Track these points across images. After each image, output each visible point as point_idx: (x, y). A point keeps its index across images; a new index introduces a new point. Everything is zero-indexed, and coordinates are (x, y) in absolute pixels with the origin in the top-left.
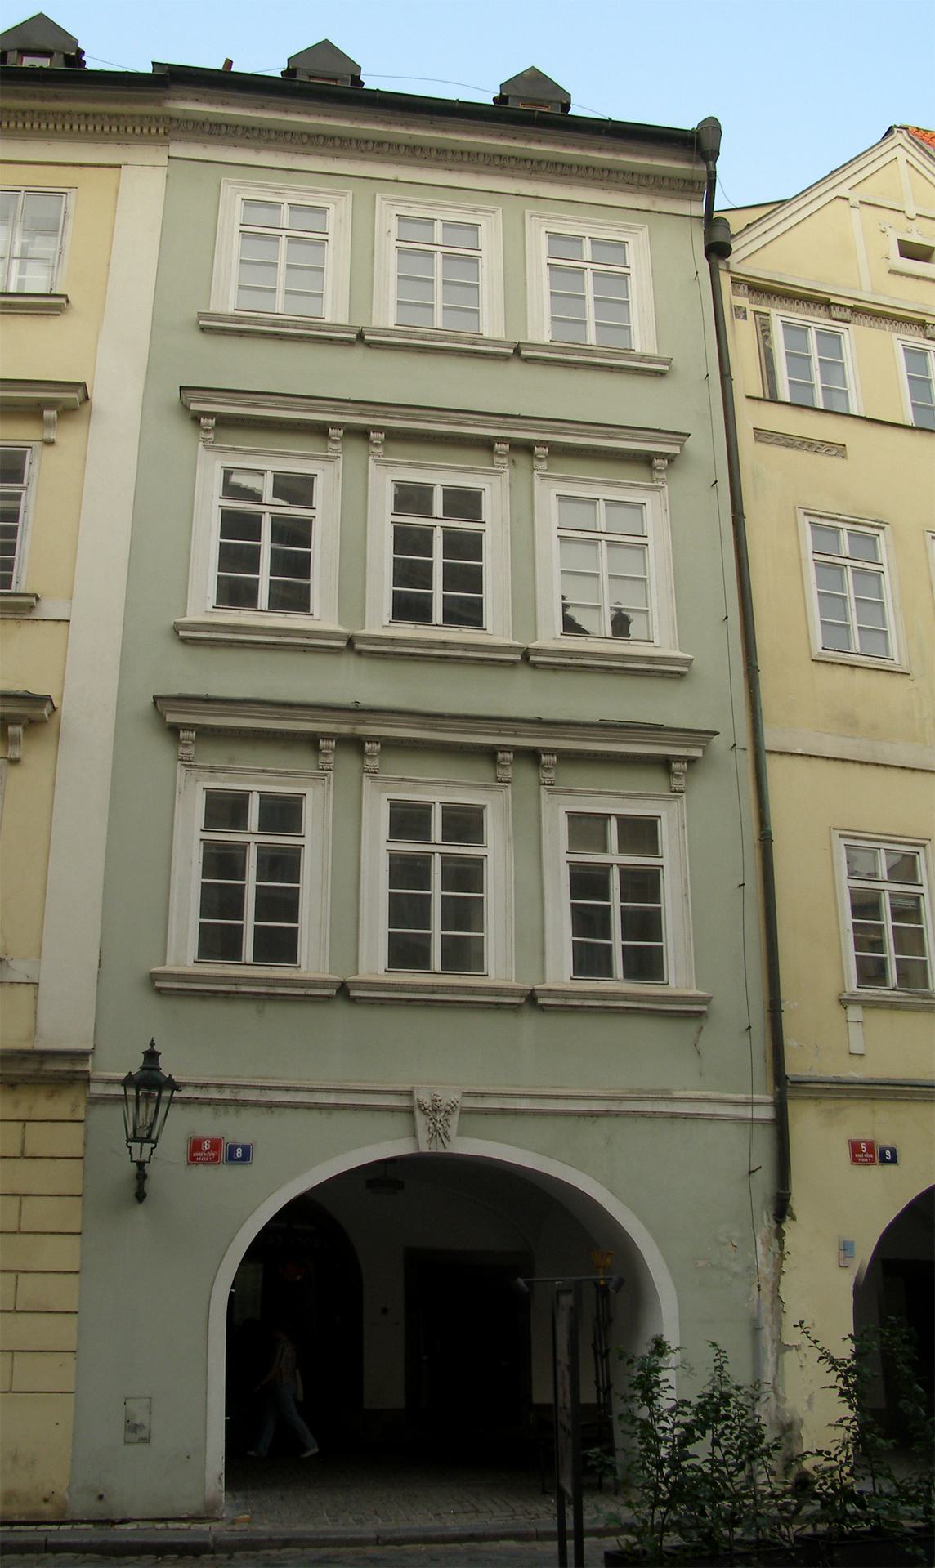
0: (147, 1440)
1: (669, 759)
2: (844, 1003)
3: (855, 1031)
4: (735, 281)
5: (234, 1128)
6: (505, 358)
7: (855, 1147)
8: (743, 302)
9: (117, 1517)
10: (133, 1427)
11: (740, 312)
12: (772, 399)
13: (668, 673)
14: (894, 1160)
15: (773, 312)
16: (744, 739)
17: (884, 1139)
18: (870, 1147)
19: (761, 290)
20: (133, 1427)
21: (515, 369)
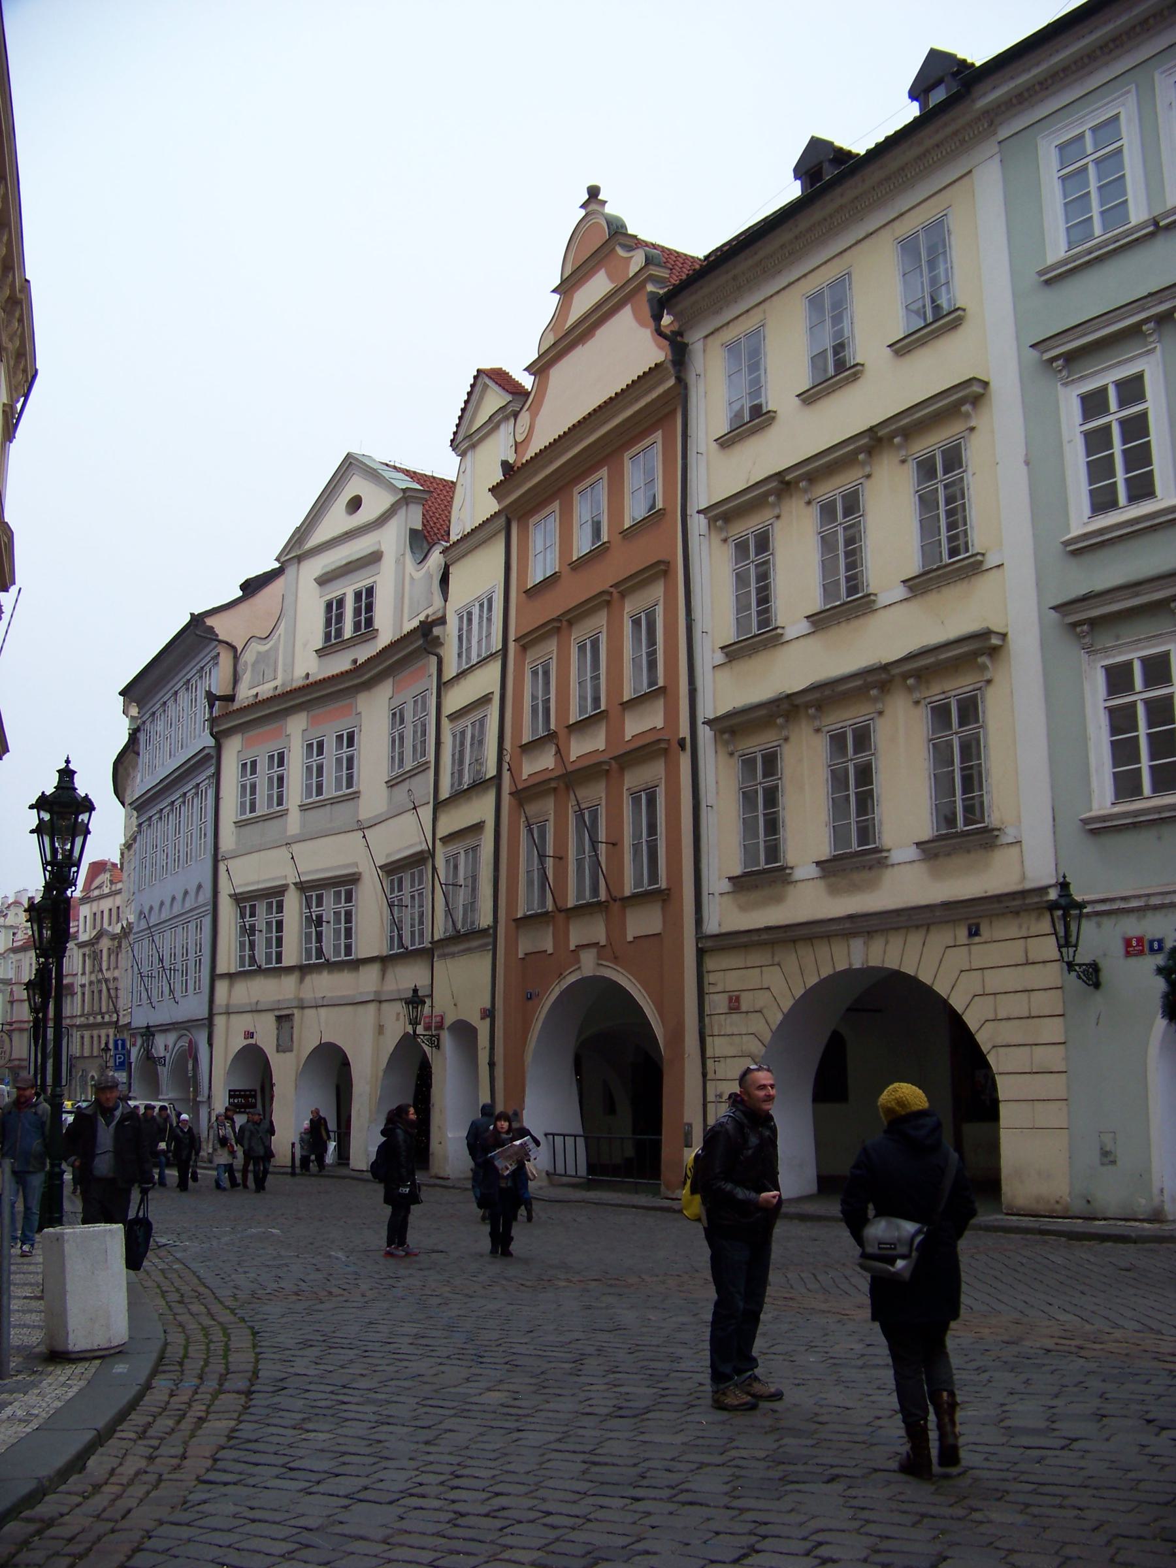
0: (1113, 1162)
9: (1100, 1216)
10: (1105, 1154)
20: (1105, 1154)
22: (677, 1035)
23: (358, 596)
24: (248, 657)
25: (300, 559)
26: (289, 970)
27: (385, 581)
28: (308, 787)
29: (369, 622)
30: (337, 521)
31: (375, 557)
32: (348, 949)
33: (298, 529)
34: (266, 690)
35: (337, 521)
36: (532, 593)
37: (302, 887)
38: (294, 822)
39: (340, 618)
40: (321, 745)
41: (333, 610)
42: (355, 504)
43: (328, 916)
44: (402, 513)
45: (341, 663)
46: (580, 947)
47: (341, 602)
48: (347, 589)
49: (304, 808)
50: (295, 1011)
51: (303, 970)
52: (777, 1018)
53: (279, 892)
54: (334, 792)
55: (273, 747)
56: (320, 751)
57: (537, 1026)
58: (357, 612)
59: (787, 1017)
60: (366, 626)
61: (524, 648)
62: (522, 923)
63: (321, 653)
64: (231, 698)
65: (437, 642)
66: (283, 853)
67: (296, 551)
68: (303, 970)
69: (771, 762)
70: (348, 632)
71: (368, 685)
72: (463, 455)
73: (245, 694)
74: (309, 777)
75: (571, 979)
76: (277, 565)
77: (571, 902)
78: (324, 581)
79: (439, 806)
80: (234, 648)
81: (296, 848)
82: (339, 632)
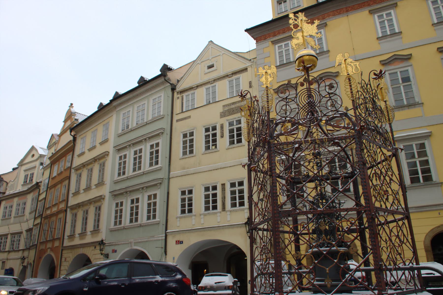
1: (157, 184)
2: (177, 218)
3: (178, 222)
4: (178, 93)
5: (115, 248)
6: (146, 125)
7: (176, 242)
8: (179, 96)
11: (178, 98)
12: (182, 112)
13: (160, 169)
14: (182, 243)
15: (184, 95)
16: (167, 177)
17: (181, 240)
18: (179, 241)
19: (182, 92)
21: (147, 126)
22: (58, 265)
23: (31, 174)
24: (9, 185)
25: (22, 165)
26: (6, 252)
27: (35, 172)
28: (16, 213)
29: (32, 180)
30: (29, 159)
31: (35, 167)
32: (18, 247)
33: (22, 160)
34: (12, 192)
35: (29, 159)
36: (53, 179)
37: (12, 234)
38: (12, 220)
39: (27, 179)
40: (19, 204)
41: (26, 177)
42: (33, 156)
43: (16, 240)
44: (40, 159)
45: (25, 188)
46: (48, 248)
47: (28, 175)
48: (29, 173)
49: (15, 217)
50: (6, 261)
51: (9, 252)
52: (70, 262)
53: (7, 235)
54: (20, 215)
55: (10, 204)
56: (19, 206)
57: (41, 264)
58: (30, 178)
59: (72, 262)
60: (31, 180)
61: (50, 189)
62: (41, 243)
63: (23, 185)
64: (4, 193)
65: (40, 186)
66: (7, 227)
67: (21, 164)
68: (9, 252)
69: (76, 215)
70: (28, 182)
71: (29, 193)
72: (49, 150)
73: (7, 193)
74: (16, 211)
75: (46, 254)
76: (17, 166)
77: (48, 239)
78: (25, 171)
79: (35, 218)
80: (7, 182)
81: (10, 226)
82: (26, 182)
